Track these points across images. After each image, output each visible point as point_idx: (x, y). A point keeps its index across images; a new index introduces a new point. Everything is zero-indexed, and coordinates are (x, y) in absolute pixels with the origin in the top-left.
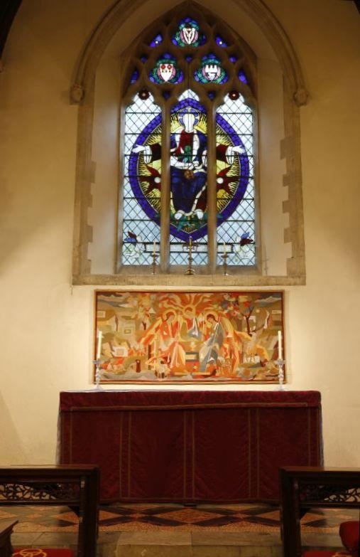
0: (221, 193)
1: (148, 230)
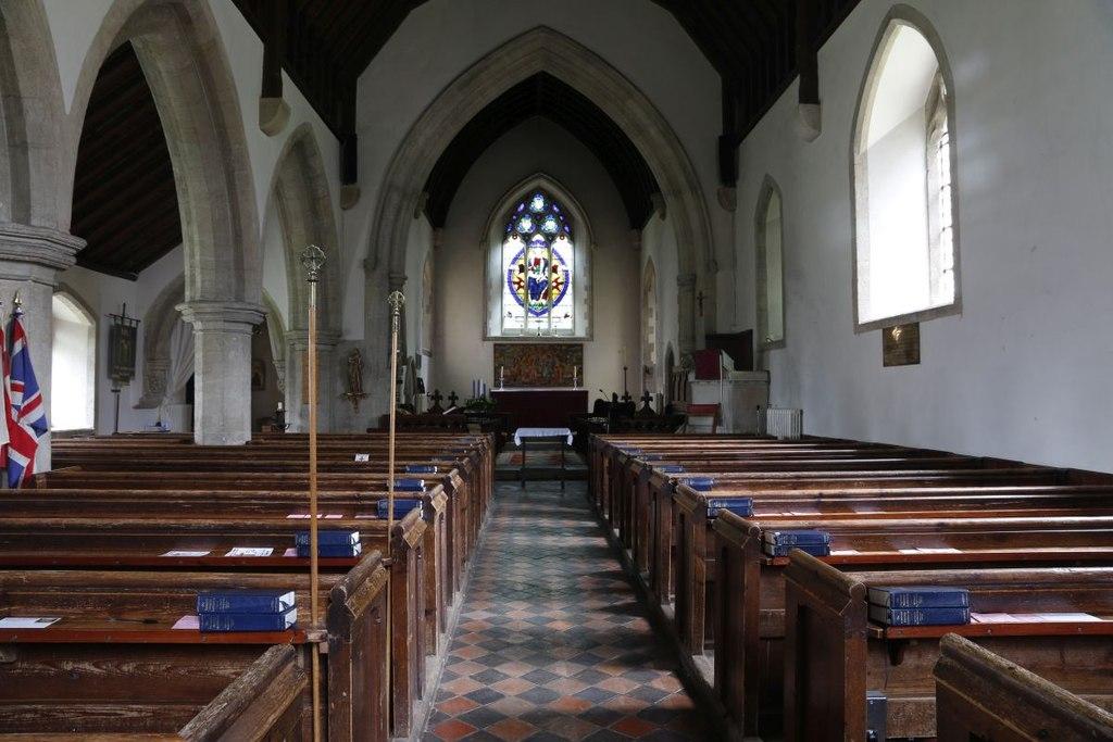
0: (555, 291)
1: (520, 311)
